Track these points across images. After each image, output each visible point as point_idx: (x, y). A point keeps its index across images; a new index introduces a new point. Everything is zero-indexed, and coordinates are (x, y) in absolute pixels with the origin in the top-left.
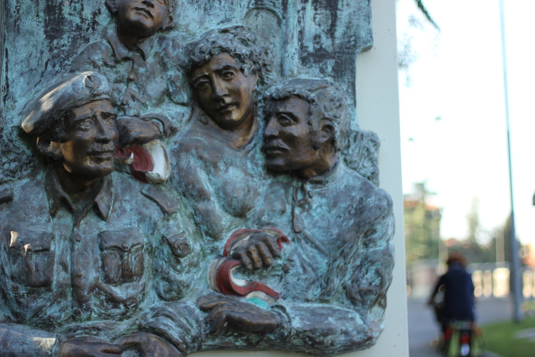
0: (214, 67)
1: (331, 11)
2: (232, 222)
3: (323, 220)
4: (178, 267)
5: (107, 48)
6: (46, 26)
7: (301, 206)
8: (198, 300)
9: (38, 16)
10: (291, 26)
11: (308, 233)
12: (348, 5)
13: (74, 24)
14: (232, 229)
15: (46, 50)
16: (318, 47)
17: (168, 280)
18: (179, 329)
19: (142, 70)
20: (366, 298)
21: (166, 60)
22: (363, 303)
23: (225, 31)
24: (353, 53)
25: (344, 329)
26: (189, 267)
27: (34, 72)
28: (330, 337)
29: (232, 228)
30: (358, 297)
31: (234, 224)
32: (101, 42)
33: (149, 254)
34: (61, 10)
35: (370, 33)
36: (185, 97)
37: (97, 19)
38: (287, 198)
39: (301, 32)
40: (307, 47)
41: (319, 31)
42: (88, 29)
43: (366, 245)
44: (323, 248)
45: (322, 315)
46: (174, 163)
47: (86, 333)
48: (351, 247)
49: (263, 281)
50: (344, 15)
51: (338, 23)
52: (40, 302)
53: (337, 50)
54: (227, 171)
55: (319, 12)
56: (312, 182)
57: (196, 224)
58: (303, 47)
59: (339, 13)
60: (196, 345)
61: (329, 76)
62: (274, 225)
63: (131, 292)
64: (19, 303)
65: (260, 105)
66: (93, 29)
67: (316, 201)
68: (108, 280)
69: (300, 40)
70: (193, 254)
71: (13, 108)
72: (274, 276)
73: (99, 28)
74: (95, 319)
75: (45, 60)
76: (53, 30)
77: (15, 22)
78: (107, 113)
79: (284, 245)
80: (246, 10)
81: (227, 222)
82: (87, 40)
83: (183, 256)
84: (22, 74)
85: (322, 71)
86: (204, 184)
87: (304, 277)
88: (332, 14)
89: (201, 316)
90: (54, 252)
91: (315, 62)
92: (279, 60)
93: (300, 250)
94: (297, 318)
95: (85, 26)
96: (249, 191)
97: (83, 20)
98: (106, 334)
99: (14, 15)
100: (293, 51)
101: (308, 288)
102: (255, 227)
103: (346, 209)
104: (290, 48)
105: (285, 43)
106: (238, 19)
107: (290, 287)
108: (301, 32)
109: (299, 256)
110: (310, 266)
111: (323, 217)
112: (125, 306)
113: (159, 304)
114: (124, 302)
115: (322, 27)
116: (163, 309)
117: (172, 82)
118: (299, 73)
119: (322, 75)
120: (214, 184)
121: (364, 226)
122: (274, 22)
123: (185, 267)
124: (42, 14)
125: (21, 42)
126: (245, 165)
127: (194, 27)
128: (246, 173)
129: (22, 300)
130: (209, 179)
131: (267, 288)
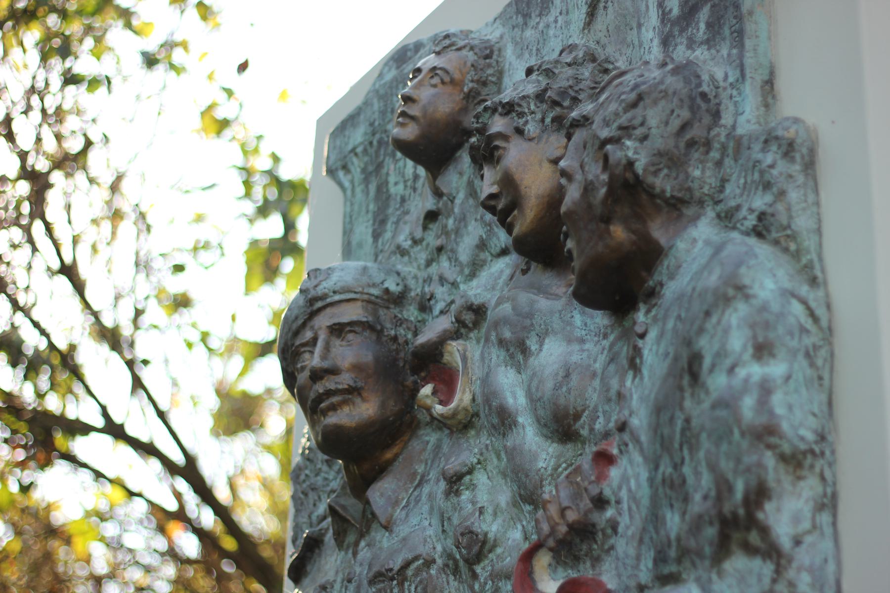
14: (562, 473)
26: (493, 582)
29: (560, 469)
31: (562, 460)
33: (455, 576)
48: (672, 419)
70: (499, 550)
78: (335, 324)
81: (550, 461)
86: (508, 394)
96: (567, 375)
100: (651, 35)
104: (646, 33)
123: (486, 583)
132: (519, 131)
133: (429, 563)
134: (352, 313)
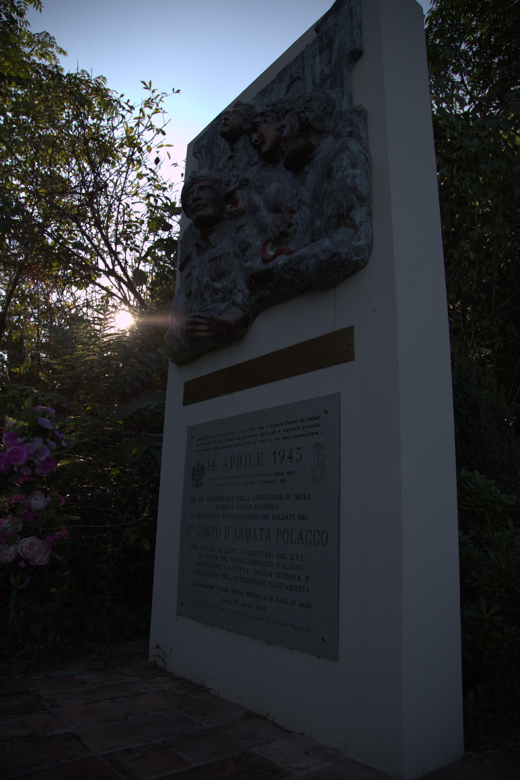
25: (313, 253)
36: (256, 159)
68: (213, 280)
70: (253, 247)
112: (222, 292)
132: (265, 121)
133: (229, 254)
134: (207, 183)
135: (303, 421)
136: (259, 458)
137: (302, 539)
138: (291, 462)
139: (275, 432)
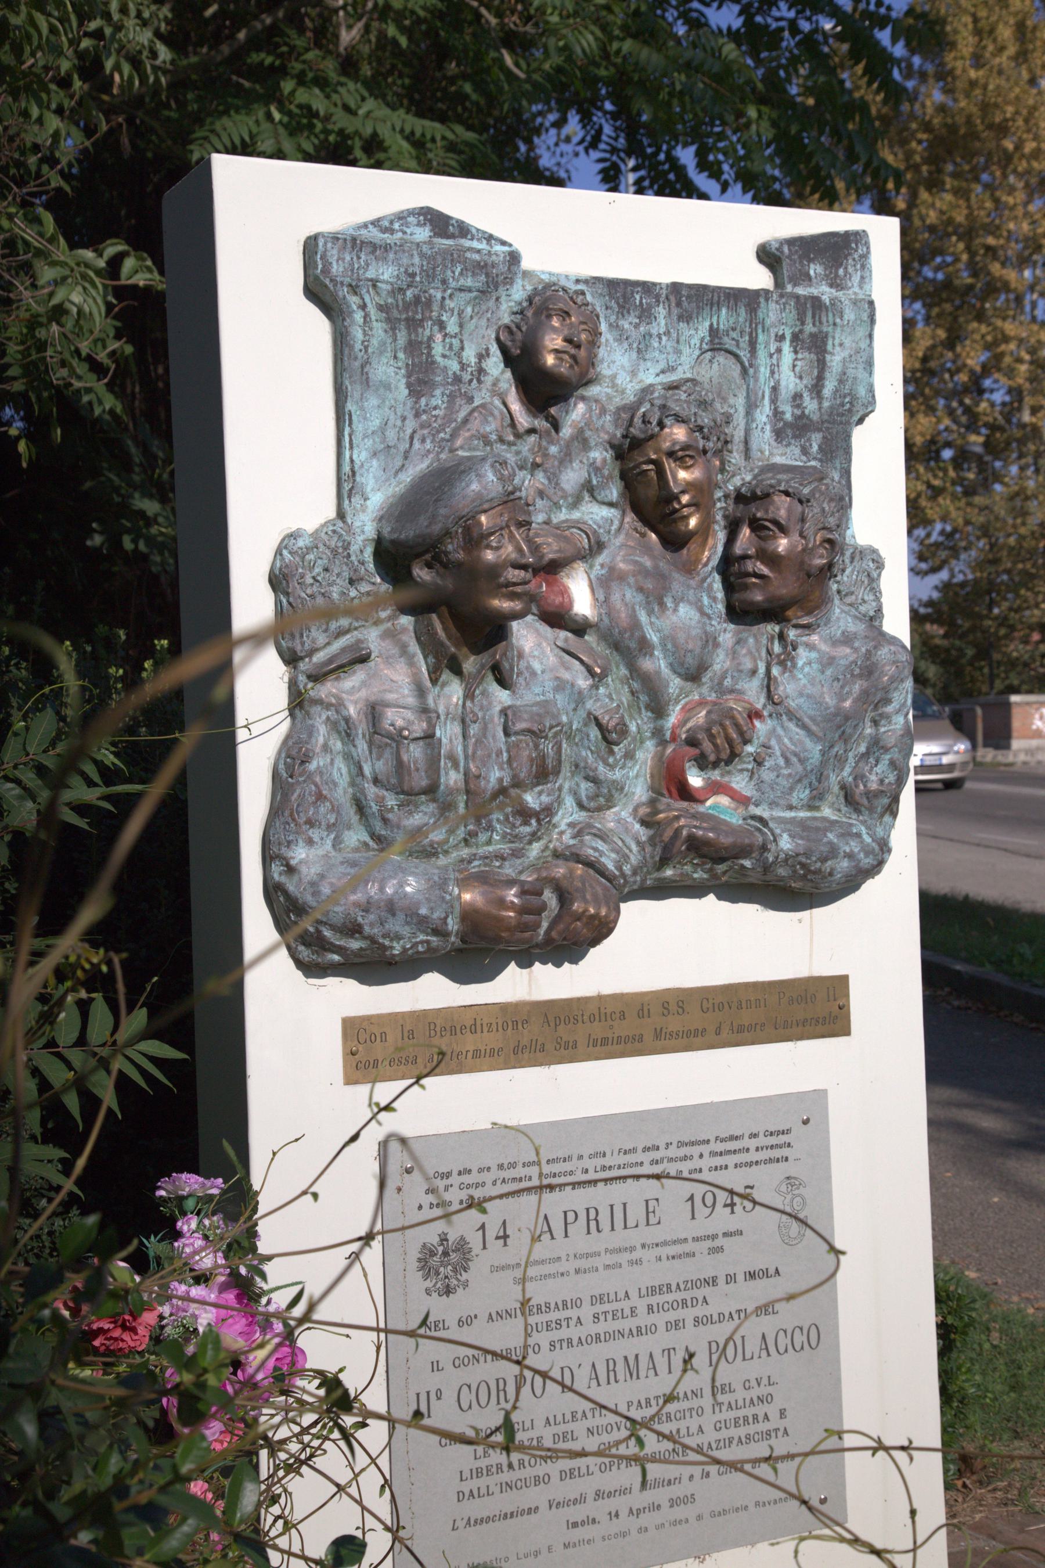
0: (666, 445)
1: (817, 354)
2: (681, 689)
3: (813, 685)
4: (611, 760)
5: (502, 413)
6: (409, 376)
7: (782, 663)
8: (635, 810)
9: (395, 357)
10: (762, 380)
11: (793, 704)
12: (841, 345)
13: (450, 373)
15: (410, 415)
16: (798, 412)
17: (595, 780)
18: (613, 855)
19: (553, 449)
20: (876, 802)
21: (588, 433)
22: (871, 810)
23: (673, 387)
24: (848, 423)
25: (848, 850)
27: (393, 450)
28: (829, 863)
30: (865, 802)
32: (492, 403)
34: (430, 348)
35: (871, 390)
36: (614, 492)
37: (484, 365)
38: (758, 650)
39: (775, 389)
40: (783, 413)
41: (801, 386)
42: (471, 381)
43: (875, 723)
44: (814, 728)
45: (817, 829)
46: (602, 598)
47: (486, 865)
48: (856, 726)
49: (726, 779)
50: (835, 360)
51: (827, 375)
52: (416, 819)
53: (826, 417)
54: (675, 610)
55: (800, 356)
56: (796, 626)
57: (633, 693)
58: (777, 414)
59: (828, 357)
60: (638, 878)
61: (815, 459)
62: (741, 692)
63: (545, 799)
64: (385, 821)
65: (718, 505)
66: (479, 381)
67: (803, 655)
69: (774, 401)
71: (364, 508)
72: (742, 770)
73: (488, 380)
74: (498, 842)
75: (409, 431)
76: (420, 382)
77: (362, 367)
79: (757, 723)
80: (697, 352)
82: (470, 399)
83: (617, 744)
84: (375, 454)
85: (805, 451)
87: (785, 772)
88: (818, 360)
89: (643, 833)
90: (440, 740)
91: (795, 437)
92: (742, 433)
93: (780, 731)
94: (785, 836)
95: (467, 377)
97: (463, 367)
98: (511, 866)
99: (360, 355)
100: (764, 419)
101: (792, 789)
102: (713, 697)
103: (847, 667)
105: (751, 407)
106: (686, 367)
107: (765, 787)
108: (775, 389)
109: (779, 739)
110: (796, 755)
111: (812, 682)
112: (539, 821)
113: (580, 816)
114: (536, 815)
115: (805, 382)
116: (589, 826)
117: (597, 470)
118: (771, 454)
119: (804, 458)
120: (659, 631)
121: (875, 694)
122: (736, 371)
124: (401, 355)
125: (373, 401)
126: (700, 600)
127: (623, 379)
128: (703, 613)
129: (390, 816)
130: (651, 623)
131: (732, 789)
135: (754, 1136)
136: (651, 1209)
137: (767, 1349)
138: (733, 1212)
139: (691, 1157)
